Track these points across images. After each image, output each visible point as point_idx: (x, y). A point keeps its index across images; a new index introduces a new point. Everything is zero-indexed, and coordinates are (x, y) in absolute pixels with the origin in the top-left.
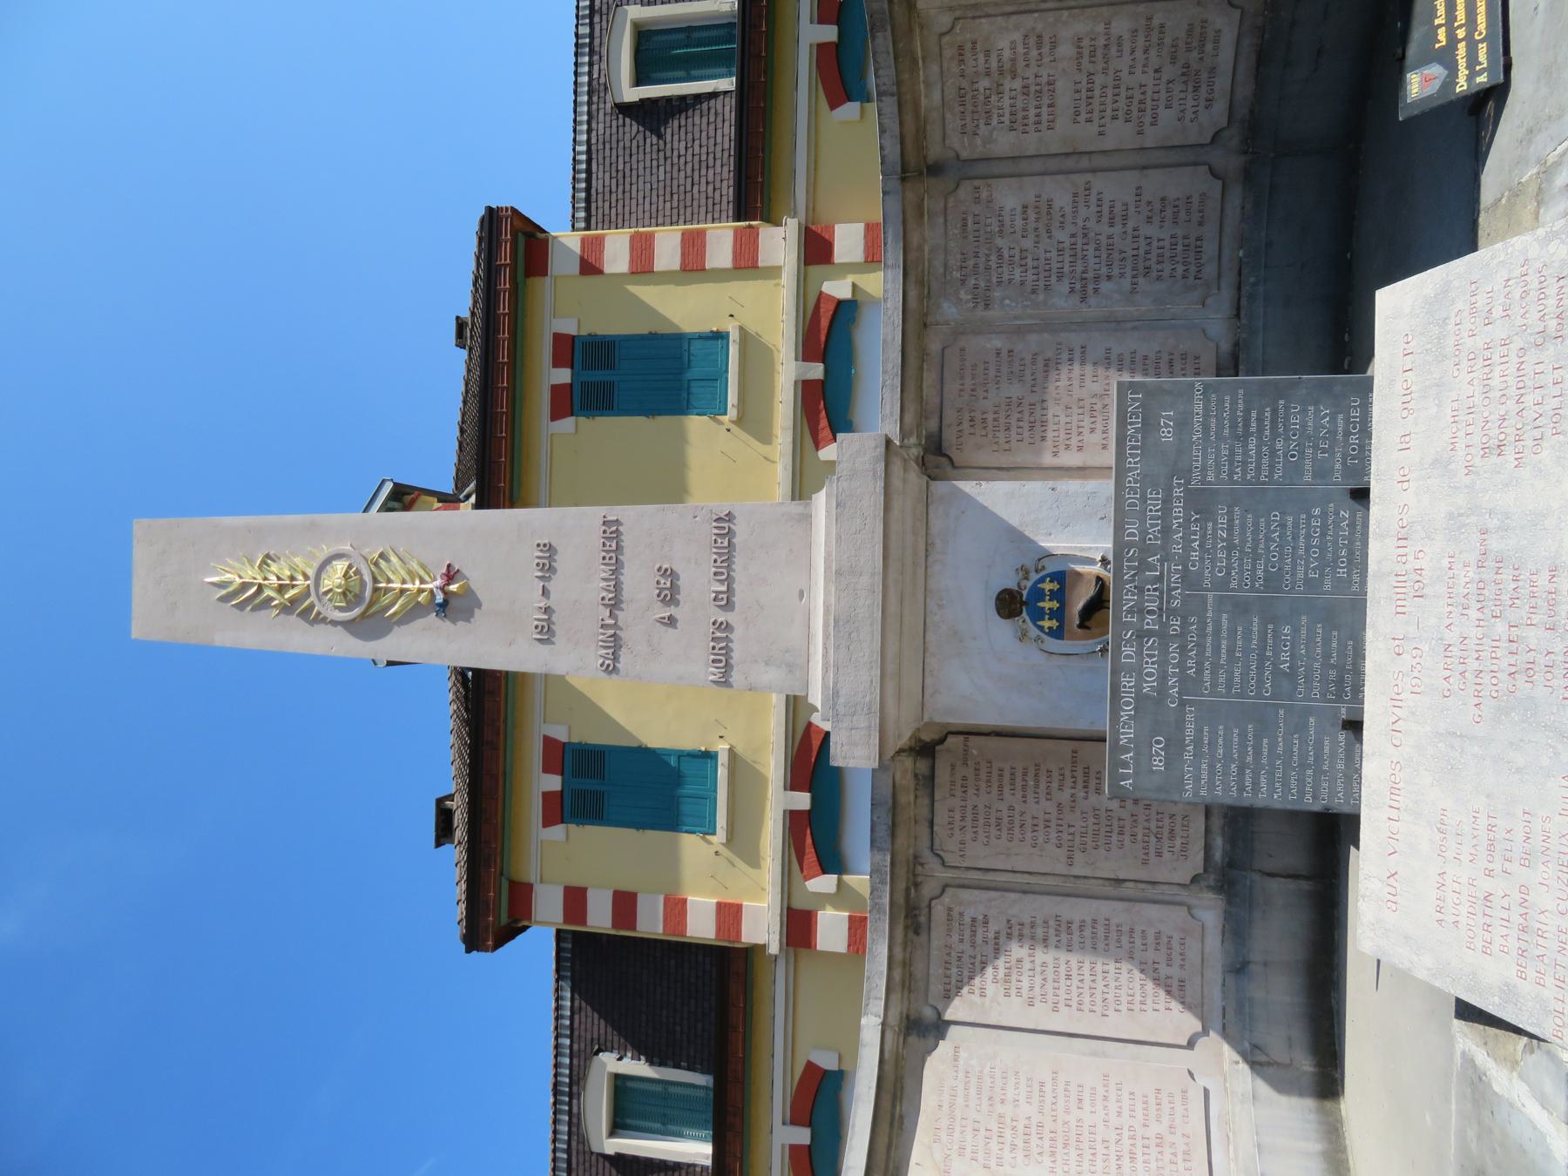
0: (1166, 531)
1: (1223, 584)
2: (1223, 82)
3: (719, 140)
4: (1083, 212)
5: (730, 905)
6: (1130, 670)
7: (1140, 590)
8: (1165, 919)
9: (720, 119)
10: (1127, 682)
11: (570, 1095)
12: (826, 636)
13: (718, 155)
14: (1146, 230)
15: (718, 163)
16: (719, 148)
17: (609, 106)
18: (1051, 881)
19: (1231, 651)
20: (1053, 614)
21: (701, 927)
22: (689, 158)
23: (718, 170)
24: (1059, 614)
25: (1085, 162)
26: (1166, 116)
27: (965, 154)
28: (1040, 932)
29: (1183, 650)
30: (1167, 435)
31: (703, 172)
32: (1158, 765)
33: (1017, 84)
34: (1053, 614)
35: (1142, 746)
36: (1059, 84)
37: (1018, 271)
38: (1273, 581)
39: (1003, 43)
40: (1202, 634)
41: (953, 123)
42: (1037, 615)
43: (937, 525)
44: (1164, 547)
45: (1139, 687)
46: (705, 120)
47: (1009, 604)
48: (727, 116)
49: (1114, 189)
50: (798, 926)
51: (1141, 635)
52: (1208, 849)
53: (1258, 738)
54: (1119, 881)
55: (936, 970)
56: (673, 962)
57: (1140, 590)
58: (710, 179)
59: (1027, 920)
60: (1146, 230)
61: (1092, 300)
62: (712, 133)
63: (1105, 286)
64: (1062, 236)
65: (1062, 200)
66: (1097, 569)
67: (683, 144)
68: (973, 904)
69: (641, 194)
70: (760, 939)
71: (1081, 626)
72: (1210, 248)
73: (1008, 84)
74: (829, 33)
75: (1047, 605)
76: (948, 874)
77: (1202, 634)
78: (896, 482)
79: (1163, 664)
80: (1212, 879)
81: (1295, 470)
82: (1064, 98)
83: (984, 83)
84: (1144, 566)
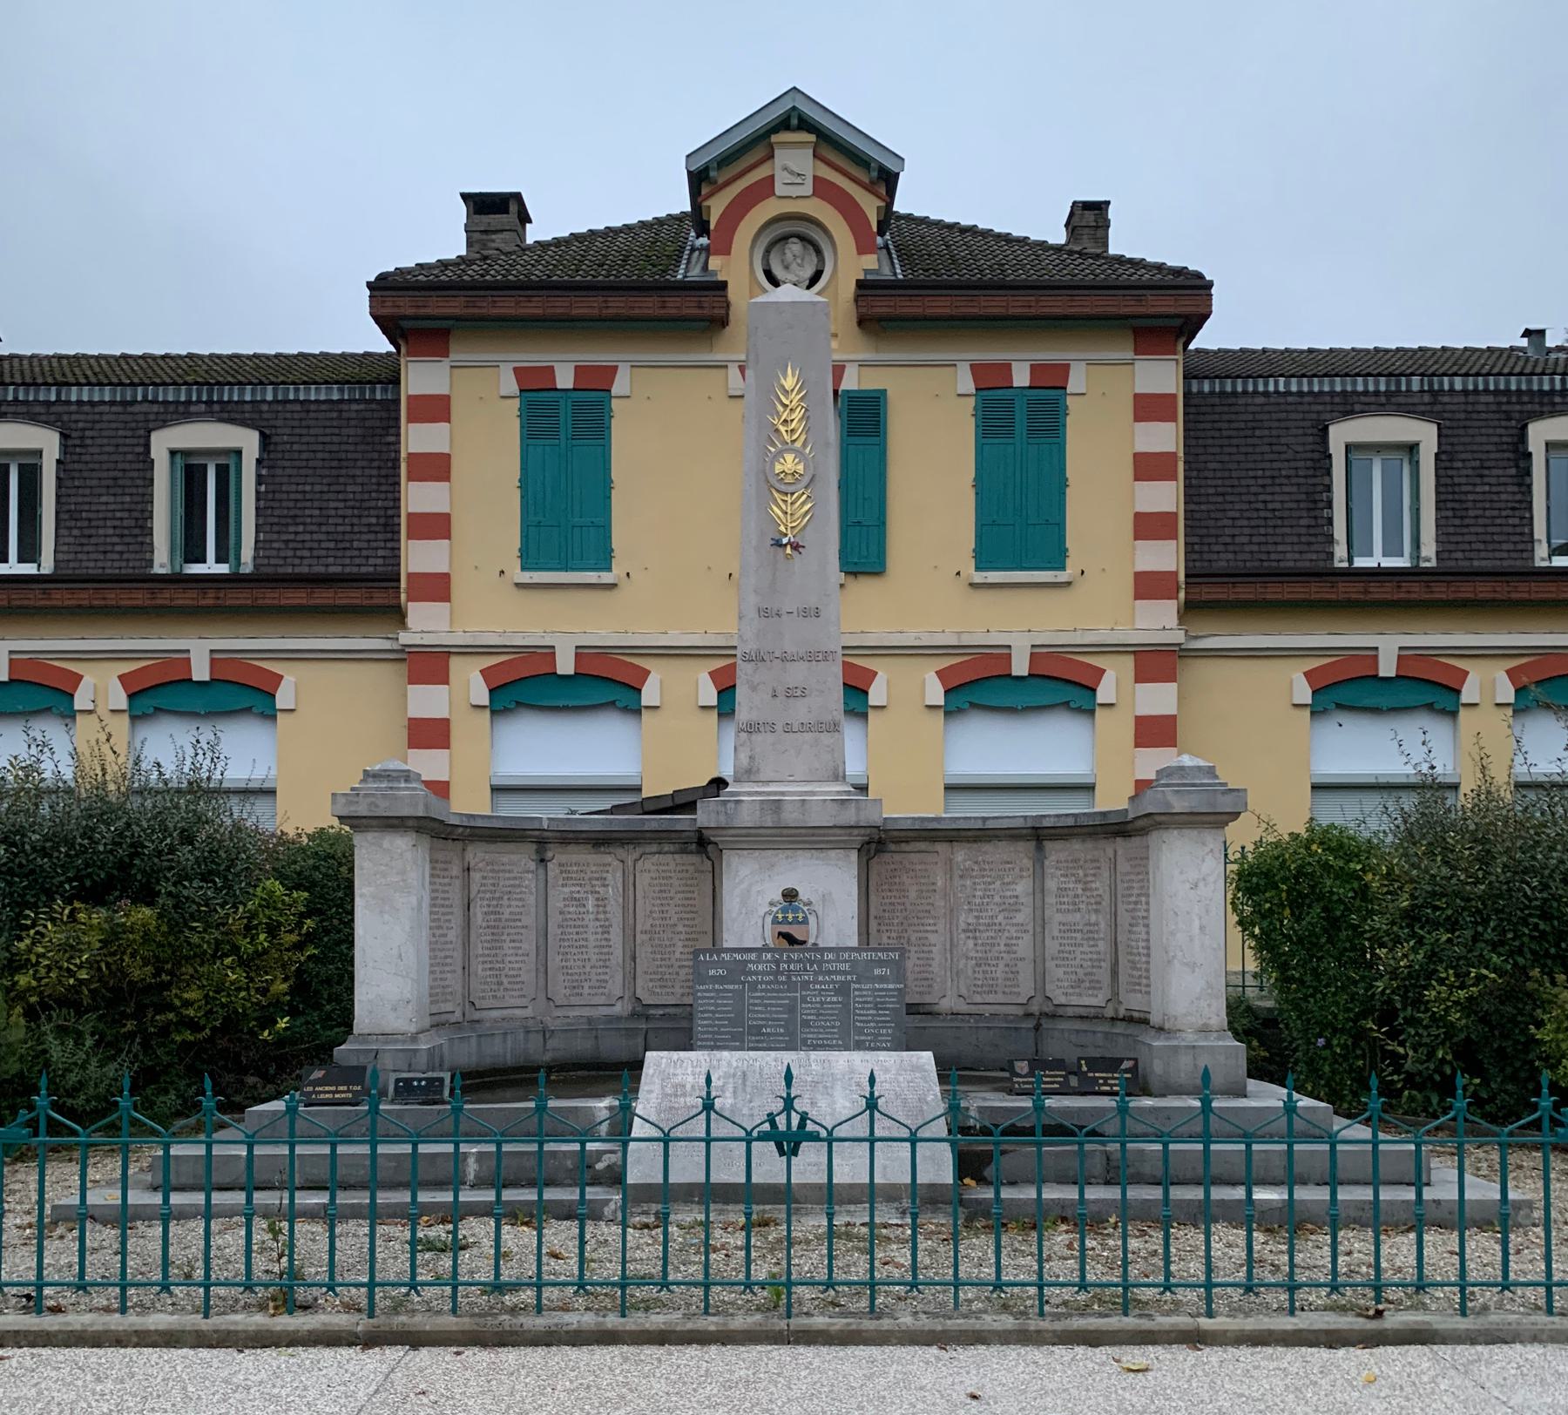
0: (830, 973)
1: (804, 1000)
2: (1075, 1000)
3: (1280, 548)
4: (1013, 929)
5: (448, 589)
6: (759, 957)
7: (799, 961)
8: (616, 986)
9: (1305, 548)
10: (753, 956)
11: (209, 402)
12: (769, 794)
13: (1263, 548)
14: (1001, 964)
15: (1255, 548)
16: (1271, 548)
17: (1323, 417)
18: (631, 922)
19: (771, 1005)
20: (785, 918)
21: (418, 557)
22: (1262, 514)
23: (1247, 548)
24: (785, 921)
25: (1039, 929)
26: (1060, 972)
27: (1047, 863)
28: (601, 916)
29: (770, 983)
30: (877, 972)
31: (1247, 531)
32: (712, 972)
33: (1080, 892)
34: (785, 918)
35: (721, 964)
36: (1078, 915)
37: (979, 893)
38: (806, 1024)
39: (1098, 884)
40: (778, 991)
41: (1062, 856)
42: (784, 911)
43: (833, 853)
44: (820, 972)
45: (751, 962)
46: (1303, 531)
47: (790, 895)
48: (1305, 556)
49: (1024, 946)
50: (429, 665)
51: (777, 963)
52: (657, 1006)
53: (728, 1019)
54: (634, 959)
55: (575, 858)
56: (374, 520)
57: (799, 961)
58: (1237, 540)
59: (608, 909)
60: (1001, 966)
61: (963, 936)
62: (1288, 539)
63: (971, 943)
64: (1000, 918)
65: (1020, 918)
66: (811, 941)
67: (1278, 506)
68: (615, 878)
69: (1227, 458)
70: (410, 621)
71: (780, 934)
72: (991, 998)
73: (1080, 886)
74: (1387, 669)
75: (790, 916)
76: (630, 863)
77: (778, 991)
78: (856, 832)
79: (763, 973)
80: (639, 1009)
81: (860, 1031)
82: (1070, 918)
83: (1081, 872)
84: (812, 963)
